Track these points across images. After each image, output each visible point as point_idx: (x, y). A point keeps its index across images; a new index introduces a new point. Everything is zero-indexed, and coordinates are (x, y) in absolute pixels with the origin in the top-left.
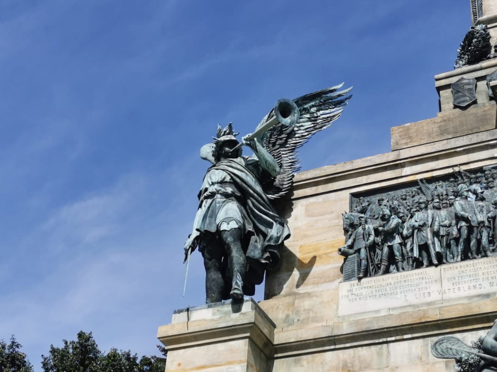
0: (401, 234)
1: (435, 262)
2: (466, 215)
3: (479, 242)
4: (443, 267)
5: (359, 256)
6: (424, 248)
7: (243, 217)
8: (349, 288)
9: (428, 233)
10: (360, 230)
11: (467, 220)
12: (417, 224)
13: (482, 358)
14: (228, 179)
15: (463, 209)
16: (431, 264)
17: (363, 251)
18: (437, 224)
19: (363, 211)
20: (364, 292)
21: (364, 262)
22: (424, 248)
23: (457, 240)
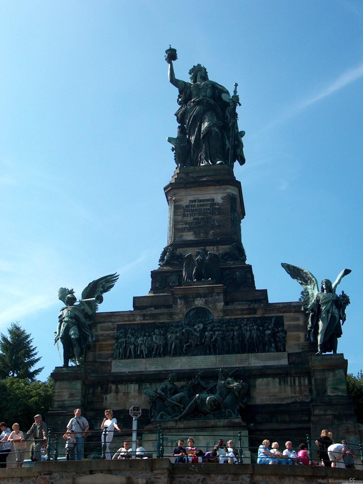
0: (134, 344)
1: (145, 357)
2: (157, 342)
3: (160, 351)
4: (147, 359)
5: (119, 351)
6: (141, 351)
7: (79, 333)
8: (115, 362)
9: (143, 347)
10: (120, 341)
11: (156, 344)
12: (140, 342)
13: (156, 396)
14: (73, 315)
15: (156, 339)
16: (143, 358)
17: (121, 349)
18: (147, 343)
19: (122, 333)
20: (121, 365)
21: (121, 353)
22: (141, 351)
23: (153, 349)
